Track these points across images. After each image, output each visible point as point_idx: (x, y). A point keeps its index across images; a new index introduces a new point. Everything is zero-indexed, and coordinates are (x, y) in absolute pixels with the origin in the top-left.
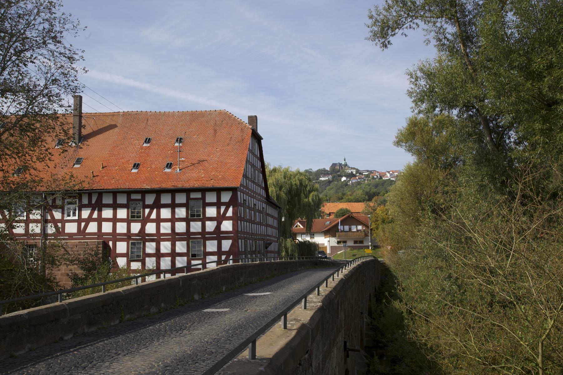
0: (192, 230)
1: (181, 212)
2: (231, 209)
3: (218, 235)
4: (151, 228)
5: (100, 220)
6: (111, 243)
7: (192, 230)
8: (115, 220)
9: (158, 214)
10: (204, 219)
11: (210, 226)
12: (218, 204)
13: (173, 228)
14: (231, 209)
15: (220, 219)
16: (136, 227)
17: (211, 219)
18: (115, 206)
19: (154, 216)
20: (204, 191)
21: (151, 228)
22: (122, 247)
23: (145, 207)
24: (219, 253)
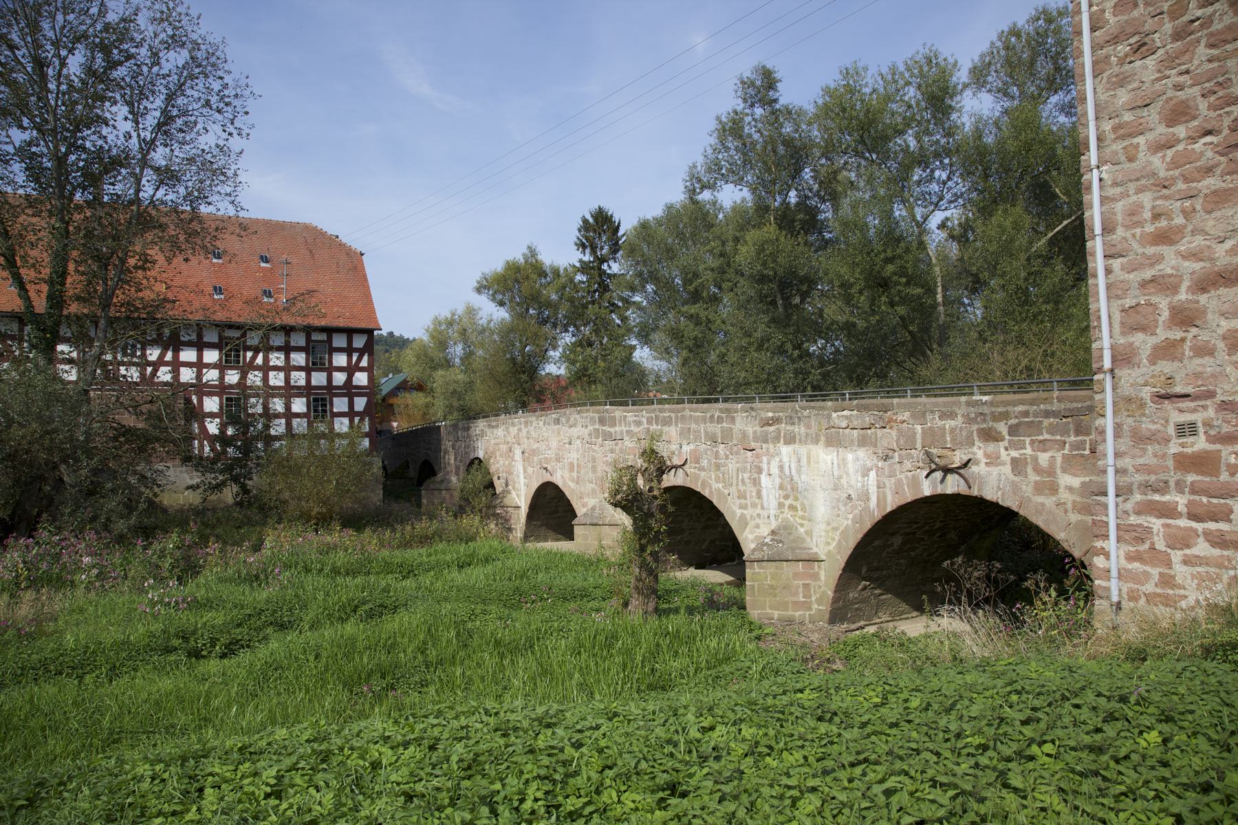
0: (314, 383)
1: (299, 358)
2: (366, 358)
3: (349, 390)
4: (255, 378)
5: (176, 365)
6: (194, 399)
7: (314, 383)
8: (199, 365)
9: (266, 360)
10: (330, 370)
11: (339, 378)
12: (349, 351)
13: (287, 379)
14: (366, 358)
15: (351, 370)
16: (232, 377)
17: (340, 369)
18: (200, 346)
19: (259, 360)
20: (330, 331)
21: (255, 378)
22: (211, 404)
23: (247, 348)
24: (351, 414)
